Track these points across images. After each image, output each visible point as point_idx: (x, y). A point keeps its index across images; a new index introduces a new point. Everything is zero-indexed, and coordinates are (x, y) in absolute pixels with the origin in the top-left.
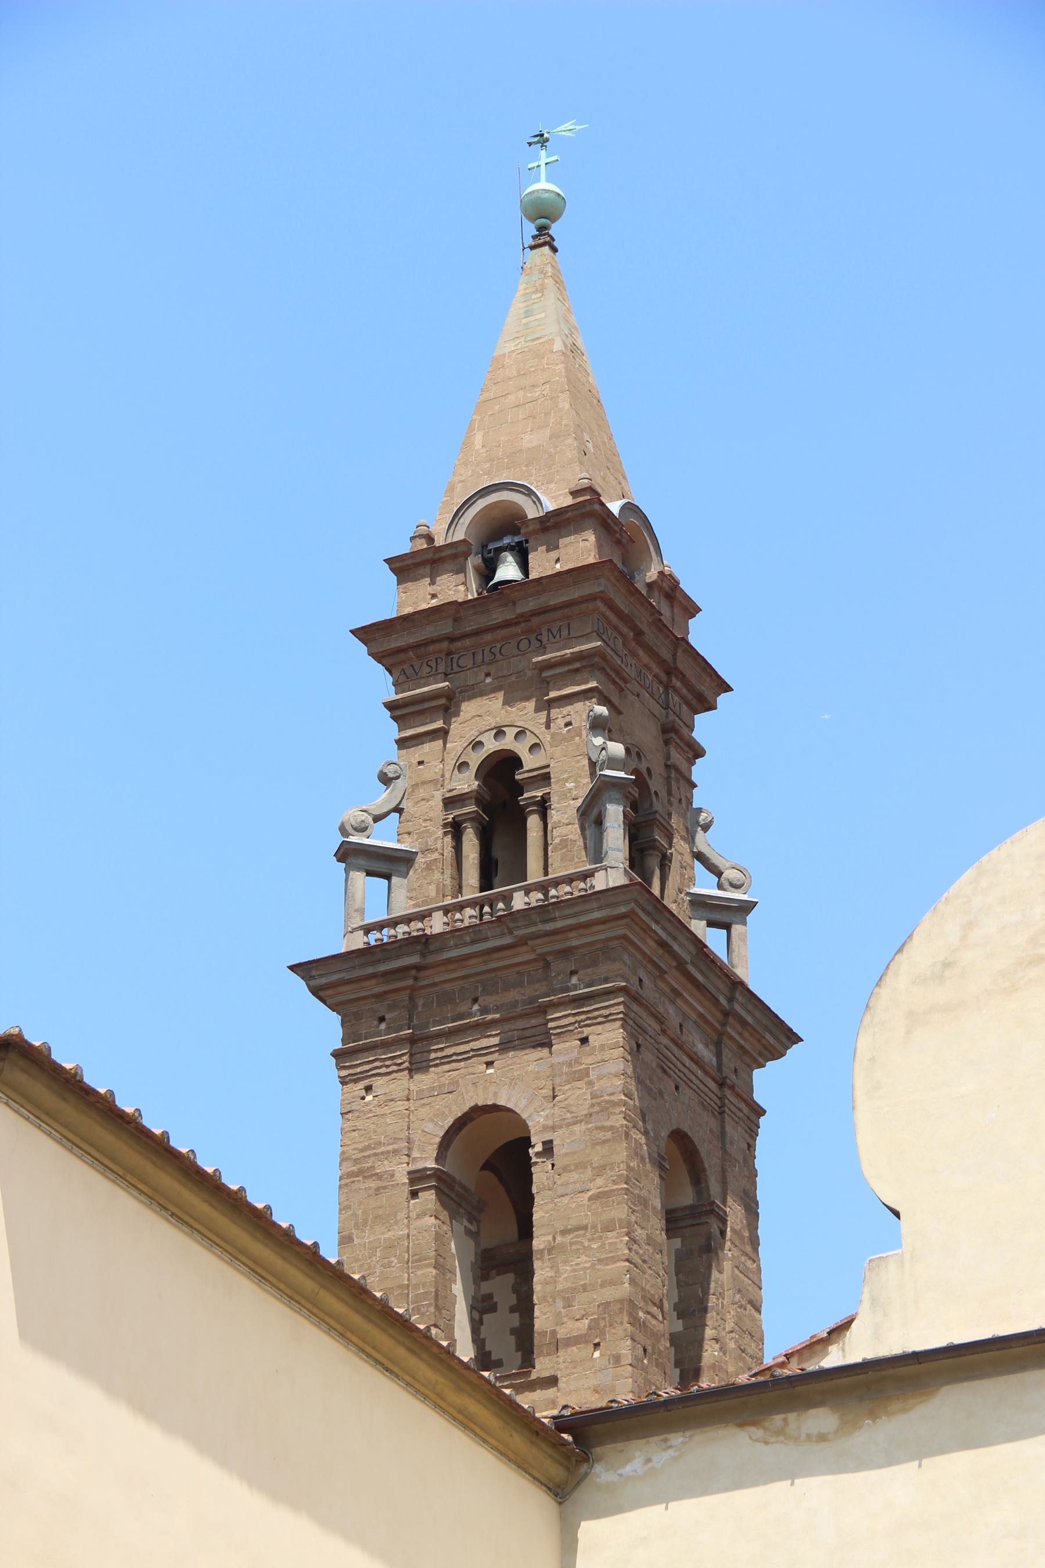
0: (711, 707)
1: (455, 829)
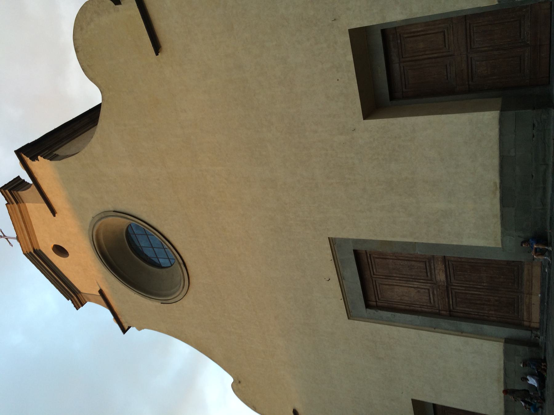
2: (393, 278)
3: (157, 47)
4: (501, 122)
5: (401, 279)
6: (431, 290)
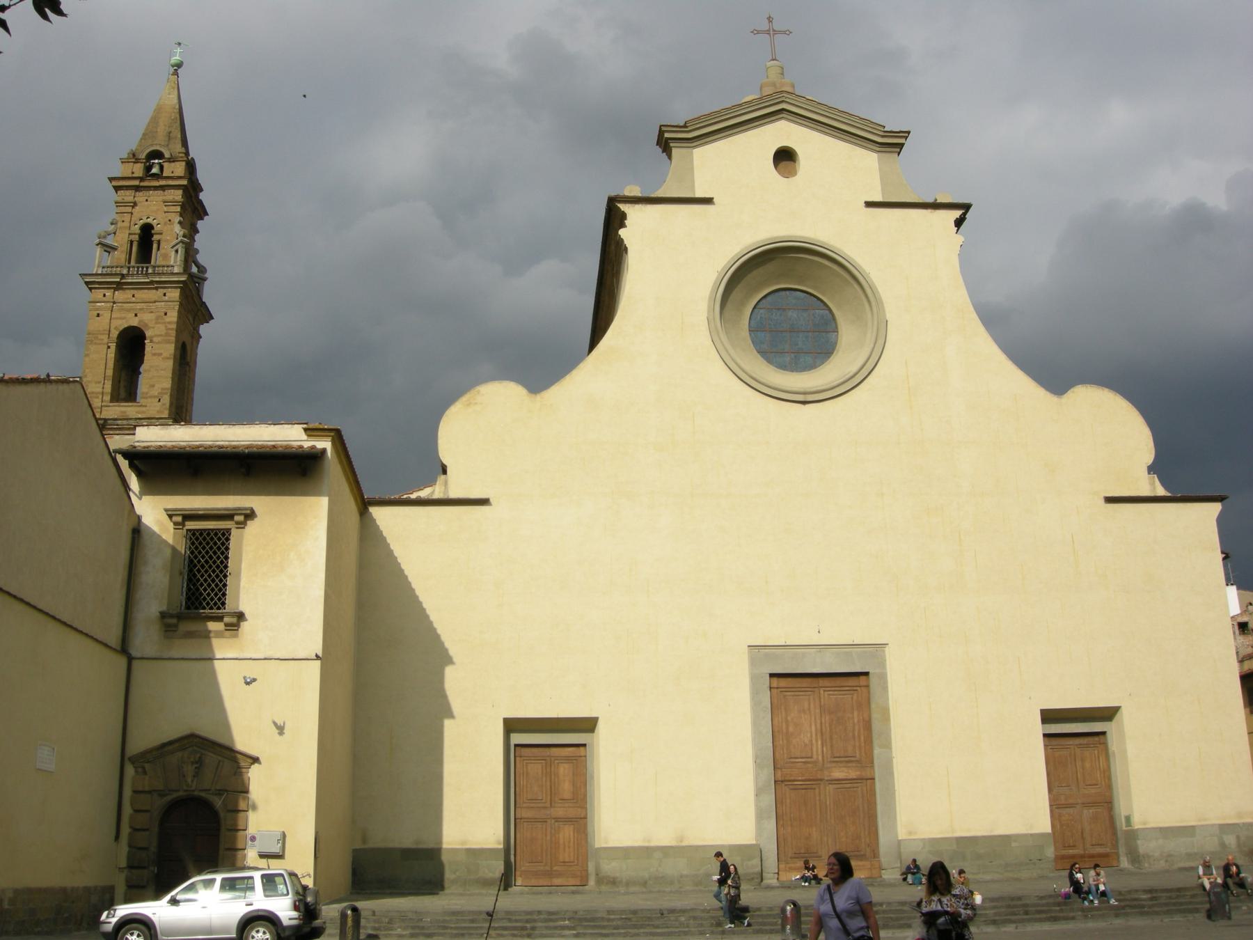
0: (202, 219)
1: (132, 242)
3: (1110, 500)
4: (1042, 835)
5: (823, 725)
6: (812, 760)
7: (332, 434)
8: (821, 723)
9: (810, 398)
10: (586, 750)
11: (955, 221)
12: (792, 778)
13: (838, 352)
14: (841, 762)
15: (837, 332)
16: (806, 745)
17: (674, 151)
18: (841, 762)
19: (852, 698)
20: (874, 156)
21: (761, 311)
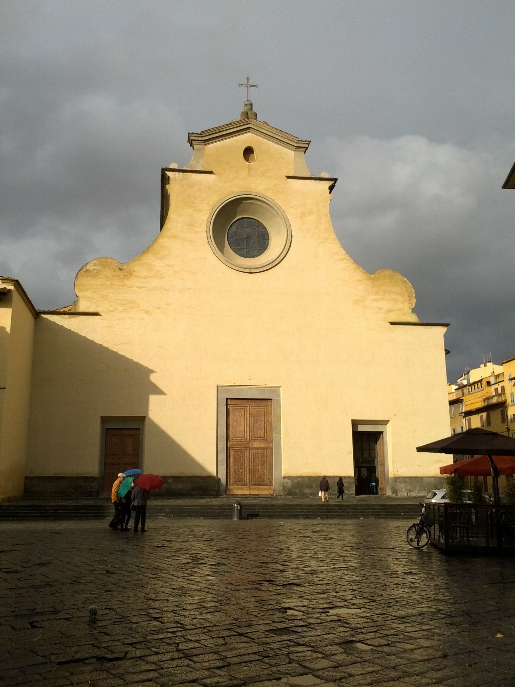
2: (250, 418)
3: (392, 323)
5: (250, 423)
6: (244, 438)
7: (14, 282)
8: (249, 421)
9: (252, 271)
10: (140, 432)
11: (329, 187)
12: (235, 446)
13: (269, 248)
14: (258, 440)
15: (269, 239)
16: (242, 431)
17: (196, 147)
18: (258, 440)
19: (264, 410)
20: (293, 152)
21: (234, 228)
